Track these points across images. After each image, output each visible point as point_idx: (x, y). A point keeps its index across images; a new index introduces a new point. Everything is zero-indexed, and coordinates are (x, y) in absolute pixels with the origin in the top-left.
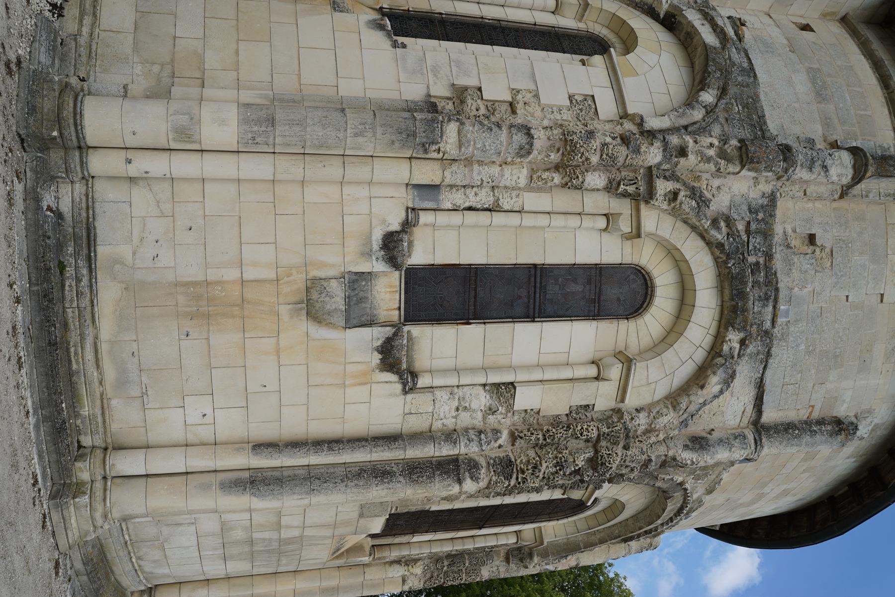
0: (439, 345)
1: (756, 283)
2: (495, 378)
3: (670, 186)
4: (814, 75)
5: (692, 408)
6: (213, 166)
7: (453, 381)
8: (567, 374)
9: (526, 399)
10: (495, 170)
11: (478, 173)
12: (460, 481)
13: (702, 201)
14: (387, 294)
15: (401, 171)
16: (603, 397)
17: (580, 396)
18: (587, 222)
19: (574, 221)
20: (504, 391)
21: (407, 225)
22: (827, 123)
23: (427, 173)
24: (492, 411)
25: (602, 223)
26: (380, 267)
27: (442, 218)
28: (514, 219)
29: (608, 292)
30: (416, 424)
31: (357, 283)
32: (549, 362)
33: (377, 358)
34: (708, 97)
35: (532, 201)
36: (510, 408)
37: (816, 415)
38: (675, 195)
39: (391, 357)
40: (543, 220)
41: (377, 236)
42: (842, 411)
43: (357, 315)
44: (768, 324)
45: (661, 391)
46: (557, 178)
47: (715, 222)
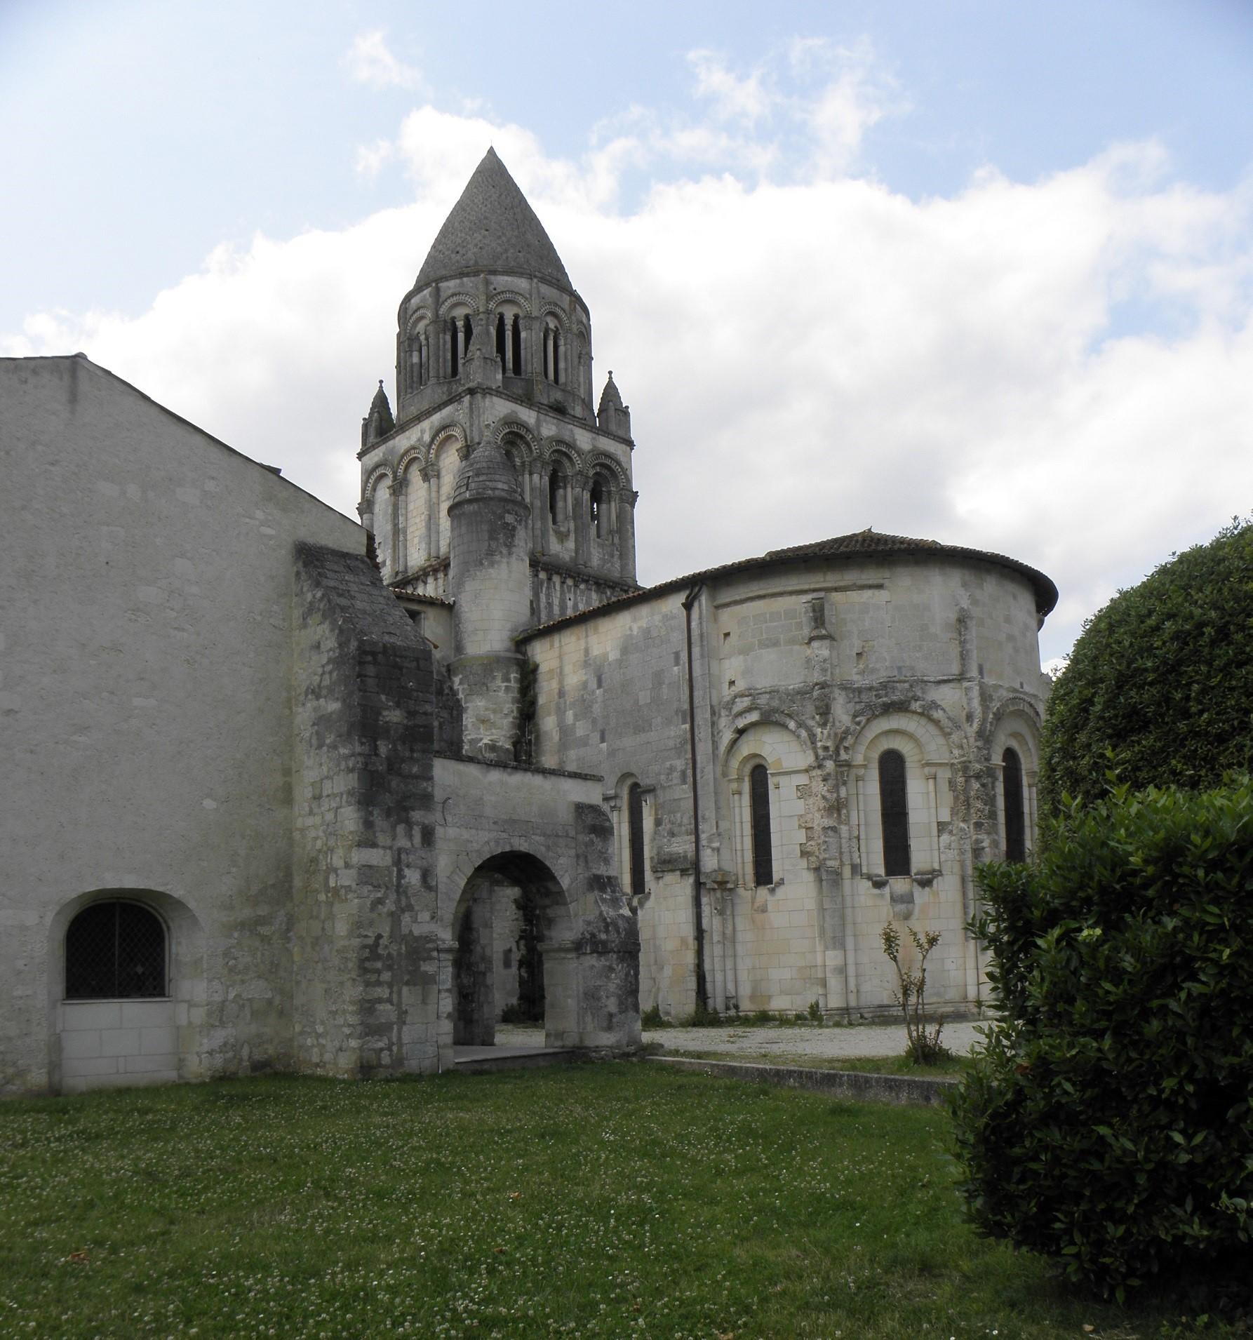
0: (921, 855)
1: (886, 696)
2: (935, 832)
3: (842, 752)
4: (764, 644)
5: (950, 725)
6: (851, 960)
7: (936, 853)
8: (933, 794)
9: (945, 816)
10: (844, 841)
11: (845, 849)
12: (983, 848)
13: (847, 732)
14: (899, 885)
15: (847, 883)
16: (944, 774)
17: (944, 786)
18: (861, 791)
19: (861, 797)
20: (942, 827)
21: (869, 877)
22: (792, 641)
23: (847, 872)
24: (951, 832)
25: (860, 783)
26: (887, 890)
27: (864, 863)
28: (862, 828)
29: (893, 771)
30: (957, 868)
31: (894, 899)
32: (925, 803)
33: (927, 889)
34: (792, 725)
35: (854, 821)
36: (949, 823)
37: (955, 635)
38: (846, 748)
39: (926, 882)
40: (862, 814)
41: (876, 891)
42: (953, 616)
43: (908, 899)
44: (906, 685)
45: (941, 741)
46: (844, 811)
47: (858, 723)
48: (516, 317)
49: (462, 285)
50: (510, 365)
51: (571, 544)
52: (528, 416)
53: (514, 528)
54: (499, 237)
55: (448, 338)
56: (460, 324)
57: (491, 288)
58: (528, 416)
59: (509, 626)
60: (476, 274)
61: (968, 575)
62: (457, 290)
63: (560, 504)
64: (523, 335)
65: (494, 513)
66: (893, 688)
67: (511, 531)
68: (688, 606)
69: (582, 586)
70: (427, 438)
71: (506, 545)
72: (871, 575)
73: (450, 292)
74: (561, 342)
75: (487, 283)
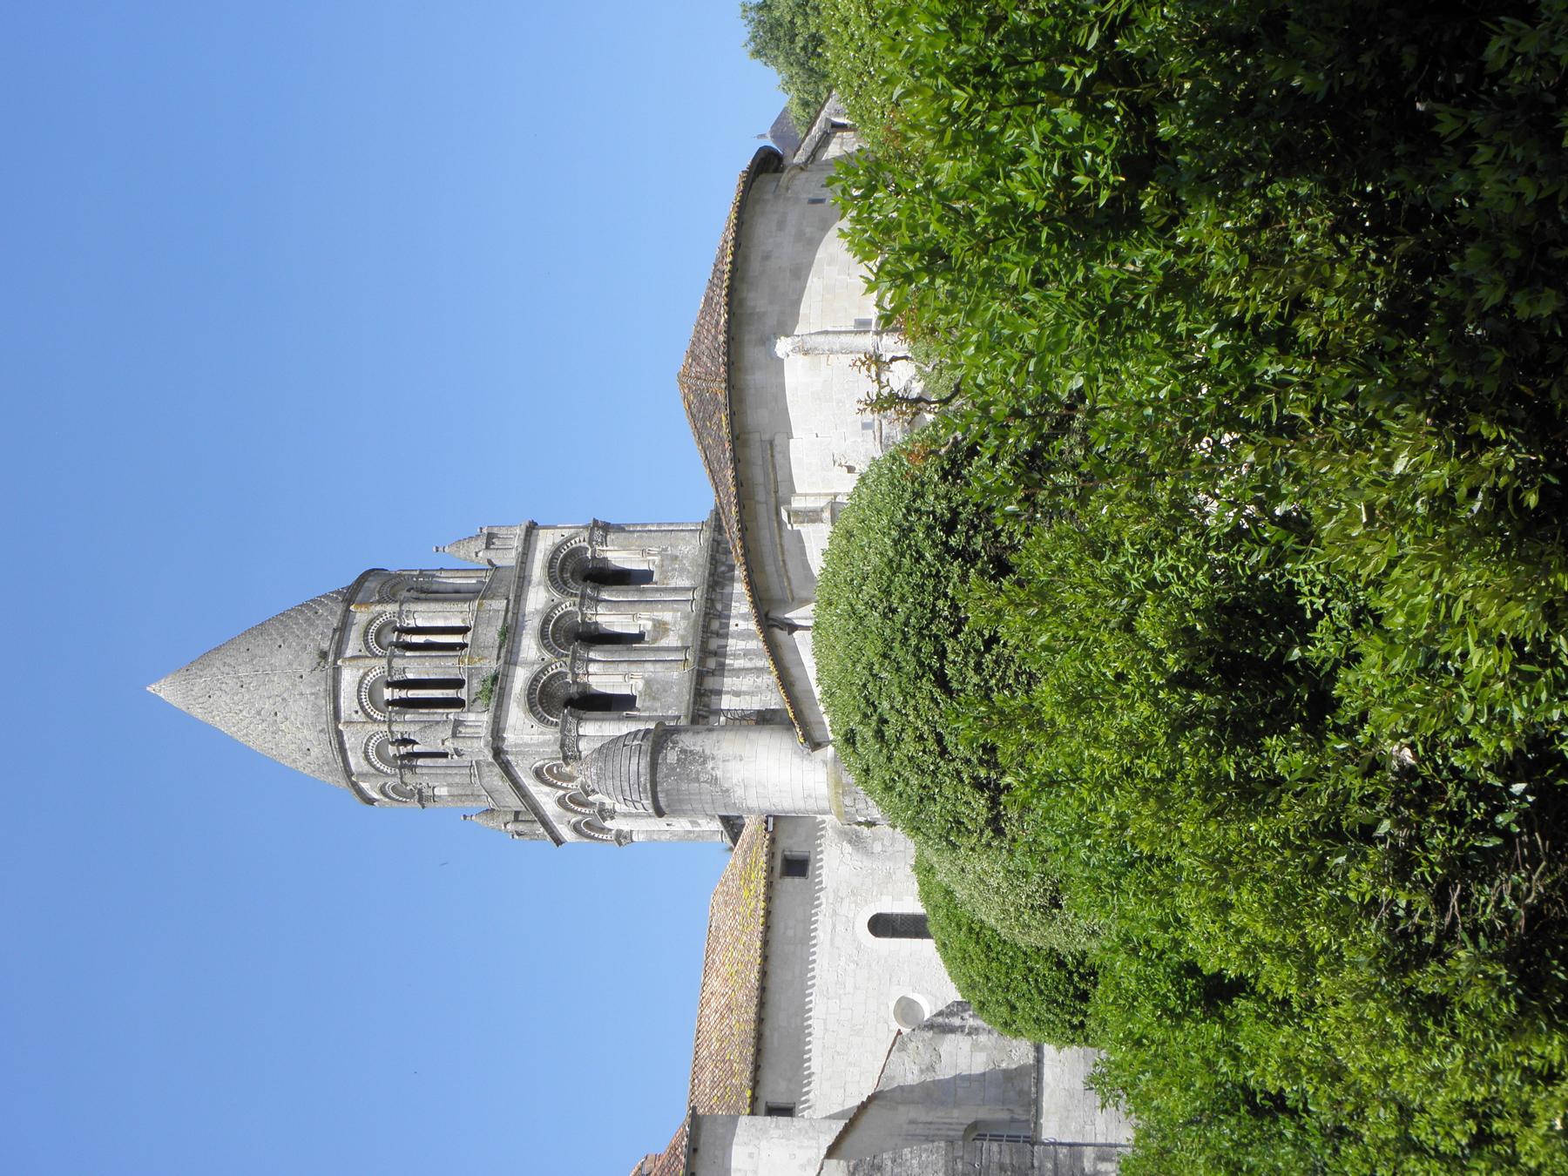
37: (823, 358)
48: (390, 685)
49: (354, 749)
50: (450, 693)
51: (667, 616)
52: (520, 679)
53: (683, 751)
55: (420, 762)
56: (403, 750)
57: (355, 717)
58: (520, 679)
59: (796, 760)
60: (339, 734)
61: (749, 337)
63: (618, 629)
64: (410, 676)
65: (667, 776)
66: (888, 438)
67: (687, 755)
68: (793, 628)
69: (719, 607)
70: (547, 789)
71: (704, 762)
72: (755, 453)
73: (363, 763)
75: (349, 723)
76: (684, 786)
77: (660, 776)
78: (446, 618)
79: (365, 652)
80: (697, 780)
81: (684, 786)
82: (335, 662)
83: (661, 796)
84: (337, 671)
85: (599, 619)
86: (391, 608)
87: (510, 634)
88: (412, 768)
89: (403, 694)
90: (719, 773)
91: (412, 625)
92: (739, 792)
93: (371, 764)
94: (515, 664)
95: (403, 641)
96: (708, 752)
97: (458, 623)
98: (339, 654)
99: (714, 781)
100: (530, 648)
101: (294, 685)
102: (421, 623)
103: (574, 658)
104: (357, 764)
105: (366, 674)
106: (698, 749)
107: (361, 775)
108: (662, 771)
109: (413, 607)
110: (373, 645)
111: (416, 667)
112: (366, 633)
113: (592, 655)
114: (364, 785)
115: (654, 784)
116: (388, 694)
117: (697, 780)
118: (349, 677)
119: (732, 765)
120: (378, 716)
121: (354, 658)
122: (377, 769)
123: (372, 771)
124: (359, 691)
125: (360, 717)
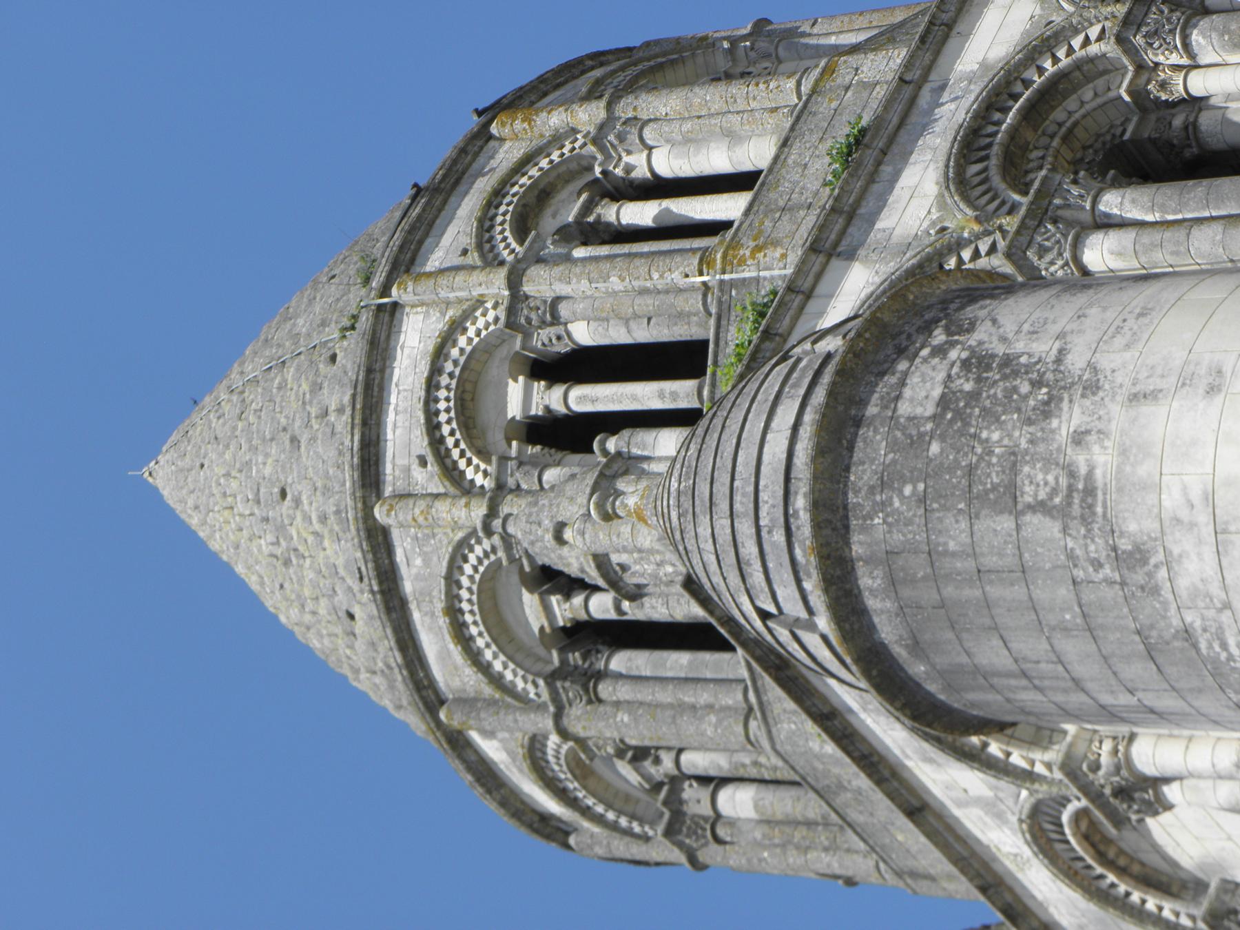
53: (978, 363)
54: (294, 440)
55: (621, 661)
60: (378, 542)
62: (443, 621)
64: (584, 334)
65: (886, 482)
71: (1047, 410)
73: (455, 651)
74: (638, 165)
76: (955, 533)
77: (862, 475)
78: (733, 137)
79: (474, 258)
80: (1008, 498)
81: (955, 533)
82: (385, 291)
83: (869, 580)
84: (389, 315)
85: (1199, 84)
86: (588, 116)
87: (870, 156)
88: (590, 679)
89: (554, 399)
90: (1101, 460)
91: (642, 172)
92: (1194, 567)
93: (474, 657)
94: (851, 256)
95: (579, 209)
96: (1076, 361)
97: (755, 153)
98: (406, 261)
99: (1079, 501)
100: (917, 201)
101: (316, 388)
102: (668, 164)
103: (1040, 214)
104: (444, 655)
105: (457, 326)
106: (1044, 348)
107: (468, 703)
108: (874, 451)
109: (650, 104)
110: (504, 233)
111: (597, 302)
112: (498, 193)
113: (1113, 202)
114: (492, 749)
115: (833, 518)
116: (519, 398)
117: (1008, 498)
118: (415, 337)
119: (1178, 422)
120: (477, 474)
121: (442, 271)
122: (496, 680)
123: (488, 691)
124: (431, 385)
125: (427, 479)
